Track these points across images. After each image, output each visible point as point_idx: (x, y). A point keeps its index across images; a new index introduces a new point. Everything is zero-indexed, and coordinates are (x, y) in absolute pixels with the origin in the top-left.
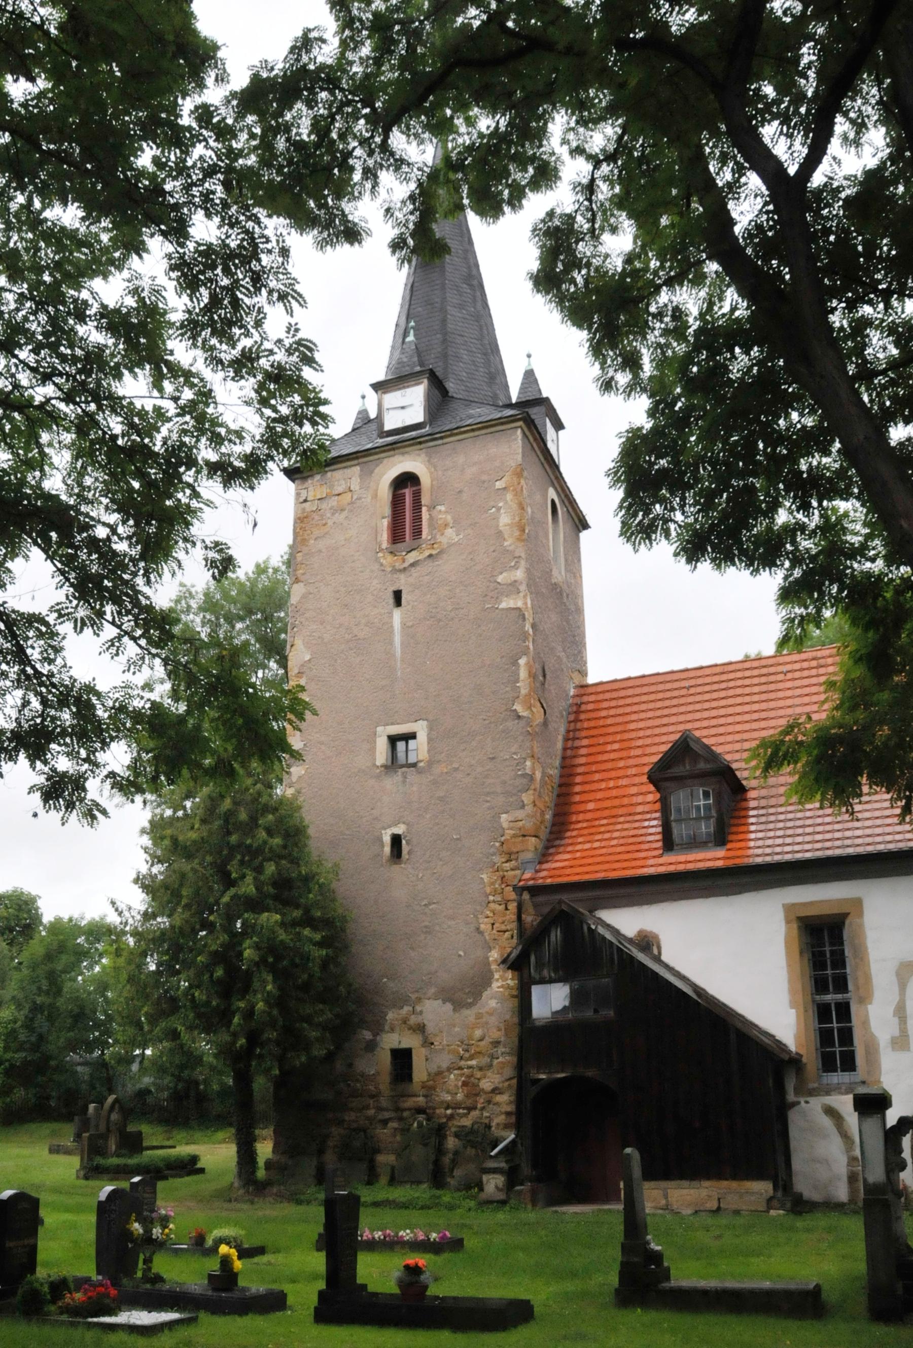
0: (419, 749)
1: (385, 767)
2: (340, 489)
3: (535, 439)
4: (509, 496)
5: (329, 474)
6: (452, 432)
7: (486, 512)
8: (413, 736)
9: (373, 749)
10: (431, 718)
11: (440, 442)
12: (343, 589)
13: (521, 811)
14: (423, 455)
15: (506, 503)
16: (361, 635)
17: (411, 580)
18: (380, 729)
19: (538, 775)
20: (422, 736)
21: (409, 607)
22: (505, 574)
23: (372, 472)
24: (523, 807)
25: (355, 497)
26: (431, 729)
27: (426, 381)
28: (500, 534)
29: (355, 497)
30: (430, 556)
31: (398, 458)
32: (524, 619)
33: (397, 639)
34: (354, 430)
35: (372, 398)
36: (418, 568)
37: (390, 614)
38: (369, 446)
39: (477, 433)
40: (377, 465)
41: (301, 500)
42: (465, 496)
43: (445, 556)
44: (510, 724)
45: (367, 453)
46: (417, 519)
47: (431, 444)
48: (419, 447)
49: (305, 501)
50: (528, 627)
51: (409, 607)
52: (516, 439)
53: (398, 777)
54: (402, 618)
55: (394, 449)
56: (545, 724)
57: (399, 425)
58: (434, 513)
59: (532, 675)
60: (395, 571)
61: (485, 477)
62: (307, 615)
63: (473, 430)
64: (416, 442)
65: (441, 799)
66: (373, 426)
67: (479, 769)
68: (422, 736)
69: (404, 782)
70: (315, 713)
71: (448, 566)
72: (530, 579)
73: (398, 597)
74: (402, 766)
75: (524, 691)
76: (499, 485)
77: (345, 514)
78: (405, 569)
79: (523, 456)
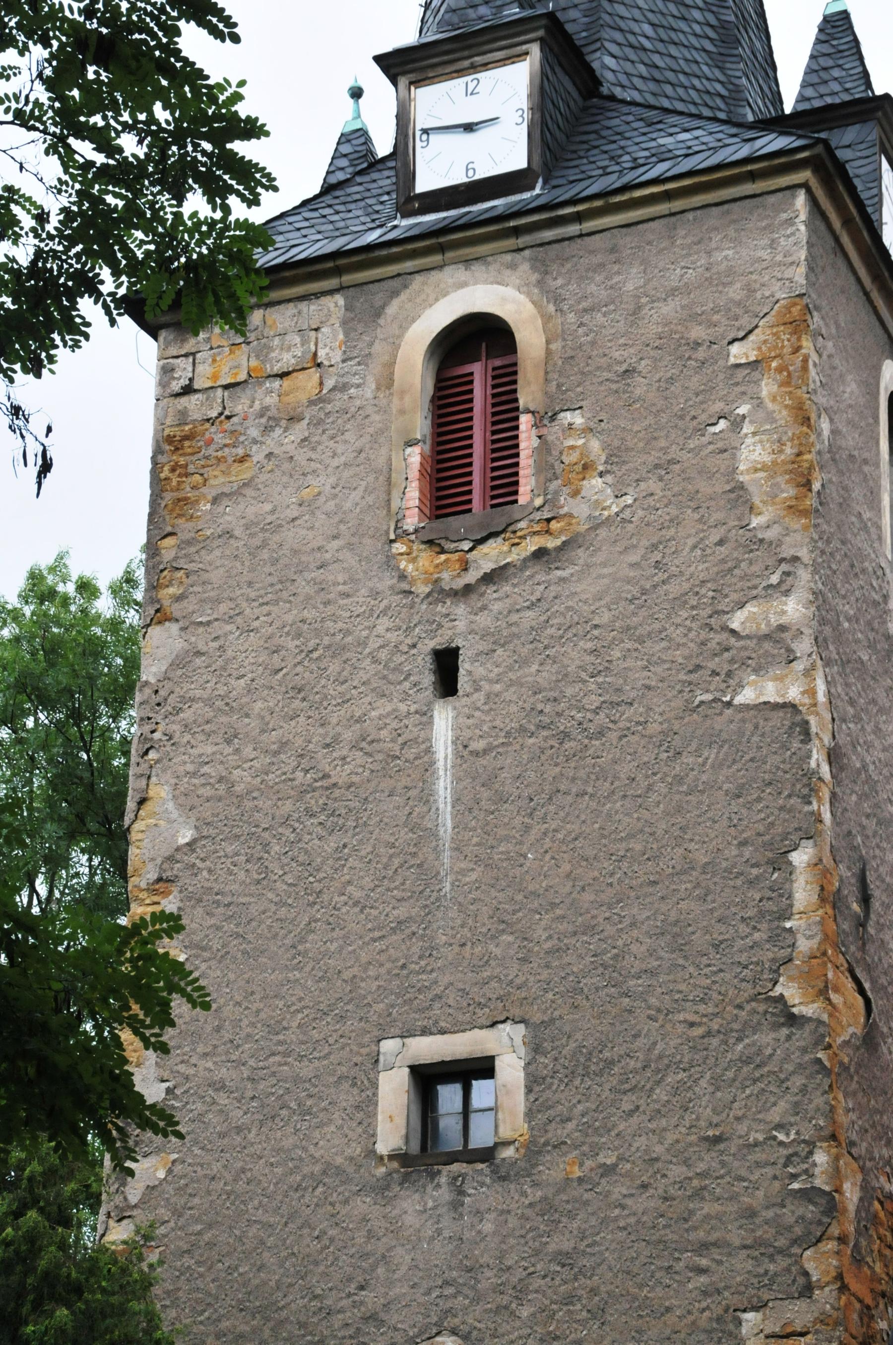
0: (502, 1105)
1: (402, 1158)
2: (286, 360)
3: (847, 222)
4: (767, 387)
6: (608, 202)
7: (701, 431)
8: (484, 1068)
9: (368, 1105)
10: (537, 1018)
11: (573, 229)
12: (291, 644)
13: (801, 1305)
14: (525, 267)
15: (759, 403)
16: (340, 775)
17: (484, 620)
18: (389, 1046)
19: (851, 1194)
20: (511, 1069)
21: (480, 697)
22: (751, 608)
23: (378, 313)
24: (807, 1291)
25: (329, 383)
26: (535, 1048)
27: (535, 50)
28: (738, 494)
29: (329, 383)
30: (540, 554)
31: (452, 274)
32: (806, 735)
33: (443, 787)
34: (328, 189)
35: (382, 93)
36: (507, 588)
37: (425, 717)
38: (372, 237)
39: (677, 205)
40: (395, 293)
41: (176, 386)
42: (640, 387)
43: (581, 554)
44: (765, 1038)
45: (369, 256)
46: (505, 448)
47: (548, 234)
48: (511, 243)
49: (188, 390)
50: (817, 759)
51: (480, 697)
52: (790, 222)
53: (440, 1192)
54: (457, 728)
55: (442, 249)
56: (870, 1040)
57: (457, 177)
58: (553, 432)
59: (830, 898)
60: (441, 594)
61: (697, 332)
62: (187, 715)
63: (668, 196)
64: (505, 230)
65: (564, 1259)
66: (385, 180)
67: (677, 1171)
68: (511, 1069)
69: (456, 1205)
70: (200, 1001)
71: (589, 585)
72: (823, 622)
74: (452, 1158)
75: (804, 945)
76: (738, 353)
77: (300, 430)
78: (468, 589)
79: (811, 269)
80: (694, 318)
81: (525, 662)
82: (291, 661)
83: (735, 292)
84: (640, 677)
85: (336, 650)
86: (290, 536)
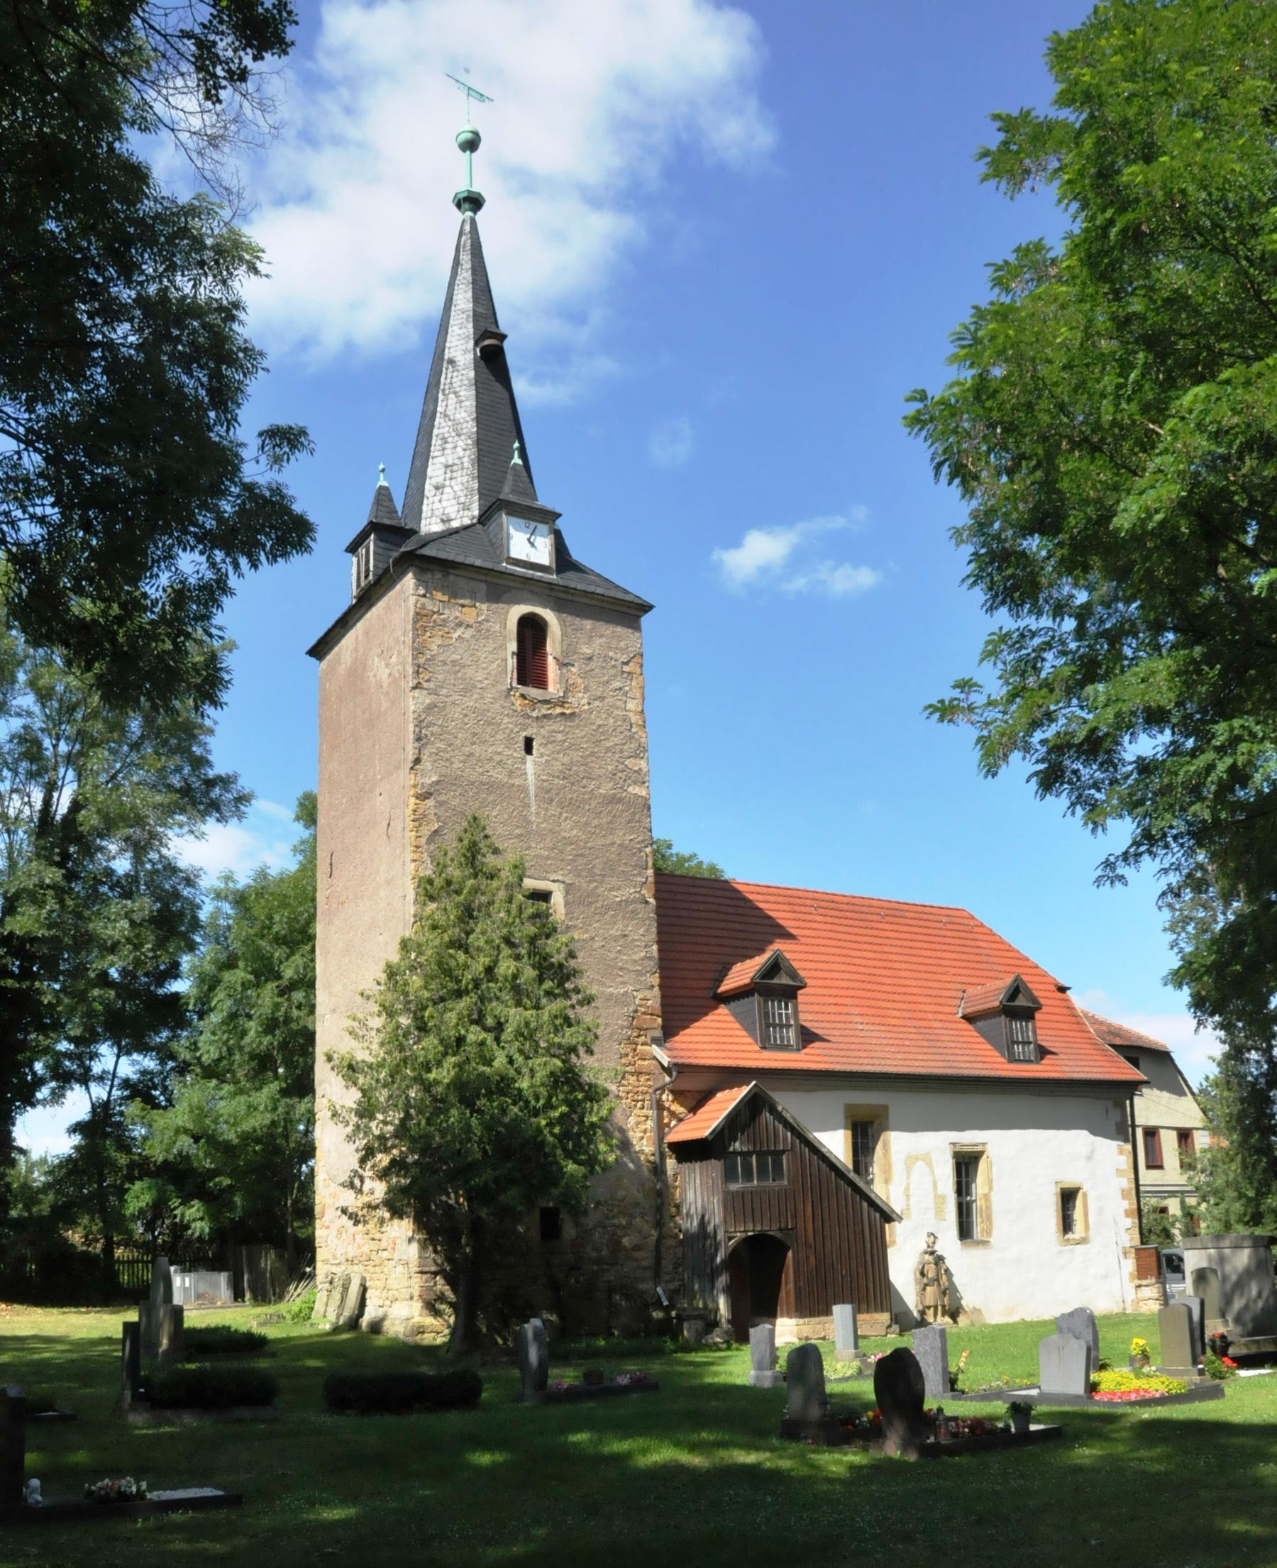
5: (452, 577)
11: (569, 597)
17: (543, 731)
26: (567, 893)
30: (563, 714)
39: (604, 605)
42: (592, 665)
47: (562, 595)
57: (524, 558)
61: (611, 654)
73: (528, 746)
77: (470, 632)
80: (609, 648)
81: (558, 753)
82: (471, 722)
83: (622, 644)
84: (598, 772)
85: (488, 723)
86: (470, 672)
